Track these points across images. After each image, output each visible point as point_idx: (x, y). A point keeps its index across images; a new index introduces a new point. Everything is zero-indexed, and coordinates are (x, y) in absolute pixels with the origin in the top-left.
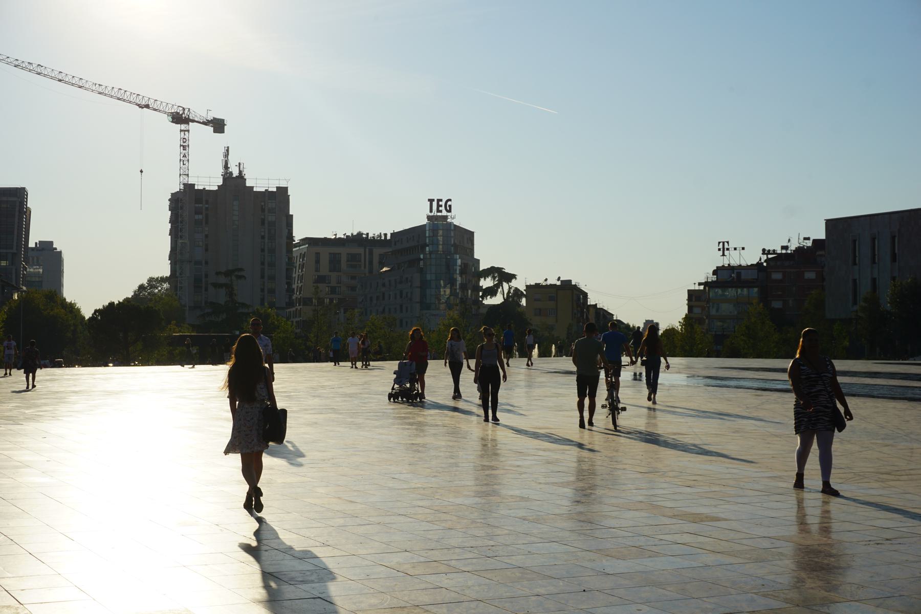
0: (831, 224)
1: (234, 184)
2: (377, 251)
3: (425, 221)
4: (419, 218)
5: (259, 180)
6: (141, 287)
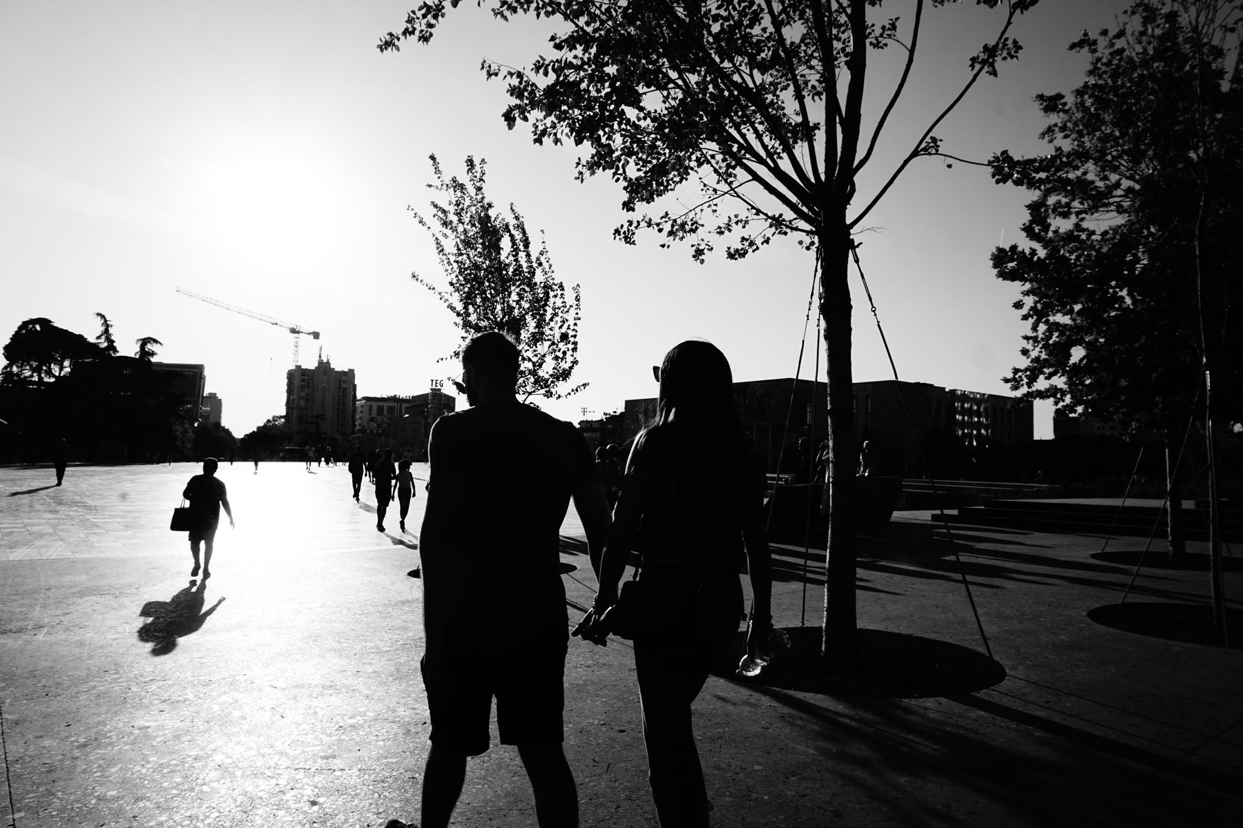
0: (628, 403)
1: (324, 367)
2: (404, 406)
3: (429, 391)
4: (425, 389)
5: (338, 365)
6: (269, 421)
